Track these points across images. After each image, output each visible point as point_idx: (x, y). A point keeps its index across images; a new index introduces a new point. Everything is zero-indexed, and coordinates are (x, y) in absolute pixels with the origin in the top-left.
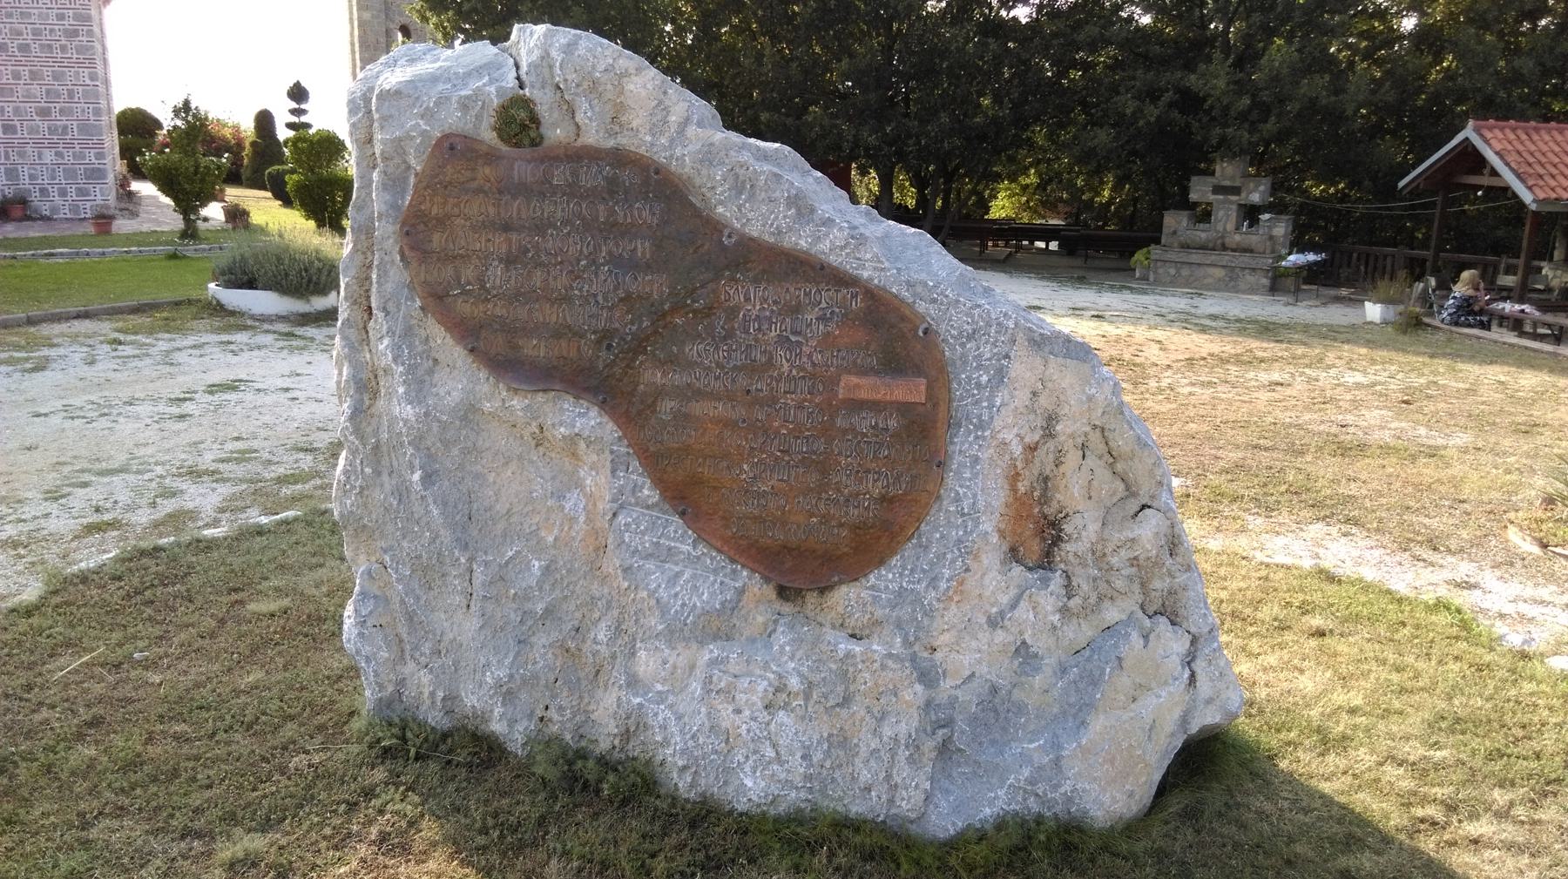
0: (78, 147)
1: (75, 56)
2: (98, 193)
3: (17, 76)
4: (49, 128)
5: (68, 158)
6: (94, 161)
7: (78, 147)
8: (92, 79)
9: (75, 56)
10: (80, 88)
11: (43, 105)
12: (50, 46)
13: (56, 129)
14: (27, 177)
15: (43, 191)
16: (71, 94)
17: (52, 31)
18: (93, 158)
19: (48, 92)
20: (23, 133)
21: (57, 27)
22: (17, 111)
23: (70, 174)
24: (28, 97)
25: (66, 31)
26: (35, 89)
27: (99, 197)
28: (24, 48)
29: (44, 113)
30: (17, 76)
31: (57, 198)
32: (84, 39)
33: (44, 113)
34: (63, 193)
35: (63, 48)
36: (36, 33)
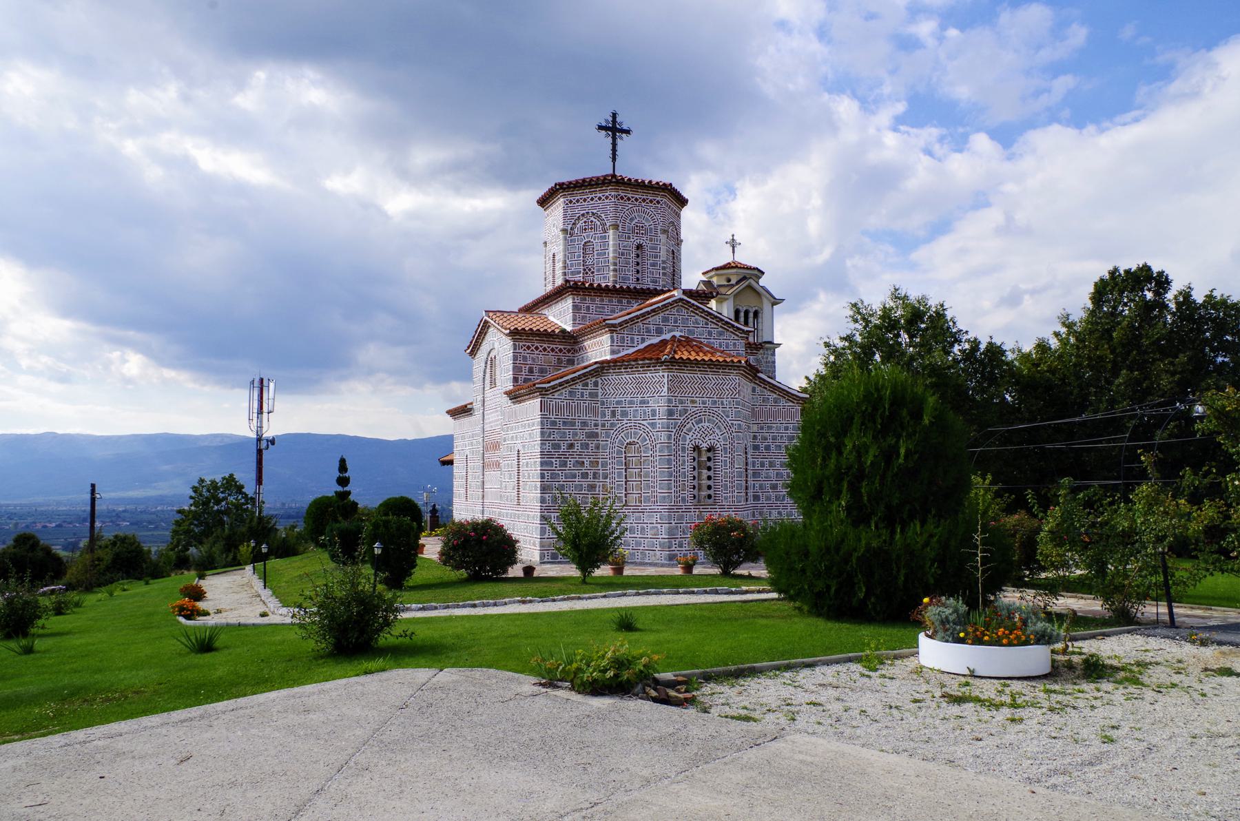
3: (762, 465)
19: (777, 474)
22: (761, 487)
28: (768, 448)
30: (762, 465)
36: (774, 438)
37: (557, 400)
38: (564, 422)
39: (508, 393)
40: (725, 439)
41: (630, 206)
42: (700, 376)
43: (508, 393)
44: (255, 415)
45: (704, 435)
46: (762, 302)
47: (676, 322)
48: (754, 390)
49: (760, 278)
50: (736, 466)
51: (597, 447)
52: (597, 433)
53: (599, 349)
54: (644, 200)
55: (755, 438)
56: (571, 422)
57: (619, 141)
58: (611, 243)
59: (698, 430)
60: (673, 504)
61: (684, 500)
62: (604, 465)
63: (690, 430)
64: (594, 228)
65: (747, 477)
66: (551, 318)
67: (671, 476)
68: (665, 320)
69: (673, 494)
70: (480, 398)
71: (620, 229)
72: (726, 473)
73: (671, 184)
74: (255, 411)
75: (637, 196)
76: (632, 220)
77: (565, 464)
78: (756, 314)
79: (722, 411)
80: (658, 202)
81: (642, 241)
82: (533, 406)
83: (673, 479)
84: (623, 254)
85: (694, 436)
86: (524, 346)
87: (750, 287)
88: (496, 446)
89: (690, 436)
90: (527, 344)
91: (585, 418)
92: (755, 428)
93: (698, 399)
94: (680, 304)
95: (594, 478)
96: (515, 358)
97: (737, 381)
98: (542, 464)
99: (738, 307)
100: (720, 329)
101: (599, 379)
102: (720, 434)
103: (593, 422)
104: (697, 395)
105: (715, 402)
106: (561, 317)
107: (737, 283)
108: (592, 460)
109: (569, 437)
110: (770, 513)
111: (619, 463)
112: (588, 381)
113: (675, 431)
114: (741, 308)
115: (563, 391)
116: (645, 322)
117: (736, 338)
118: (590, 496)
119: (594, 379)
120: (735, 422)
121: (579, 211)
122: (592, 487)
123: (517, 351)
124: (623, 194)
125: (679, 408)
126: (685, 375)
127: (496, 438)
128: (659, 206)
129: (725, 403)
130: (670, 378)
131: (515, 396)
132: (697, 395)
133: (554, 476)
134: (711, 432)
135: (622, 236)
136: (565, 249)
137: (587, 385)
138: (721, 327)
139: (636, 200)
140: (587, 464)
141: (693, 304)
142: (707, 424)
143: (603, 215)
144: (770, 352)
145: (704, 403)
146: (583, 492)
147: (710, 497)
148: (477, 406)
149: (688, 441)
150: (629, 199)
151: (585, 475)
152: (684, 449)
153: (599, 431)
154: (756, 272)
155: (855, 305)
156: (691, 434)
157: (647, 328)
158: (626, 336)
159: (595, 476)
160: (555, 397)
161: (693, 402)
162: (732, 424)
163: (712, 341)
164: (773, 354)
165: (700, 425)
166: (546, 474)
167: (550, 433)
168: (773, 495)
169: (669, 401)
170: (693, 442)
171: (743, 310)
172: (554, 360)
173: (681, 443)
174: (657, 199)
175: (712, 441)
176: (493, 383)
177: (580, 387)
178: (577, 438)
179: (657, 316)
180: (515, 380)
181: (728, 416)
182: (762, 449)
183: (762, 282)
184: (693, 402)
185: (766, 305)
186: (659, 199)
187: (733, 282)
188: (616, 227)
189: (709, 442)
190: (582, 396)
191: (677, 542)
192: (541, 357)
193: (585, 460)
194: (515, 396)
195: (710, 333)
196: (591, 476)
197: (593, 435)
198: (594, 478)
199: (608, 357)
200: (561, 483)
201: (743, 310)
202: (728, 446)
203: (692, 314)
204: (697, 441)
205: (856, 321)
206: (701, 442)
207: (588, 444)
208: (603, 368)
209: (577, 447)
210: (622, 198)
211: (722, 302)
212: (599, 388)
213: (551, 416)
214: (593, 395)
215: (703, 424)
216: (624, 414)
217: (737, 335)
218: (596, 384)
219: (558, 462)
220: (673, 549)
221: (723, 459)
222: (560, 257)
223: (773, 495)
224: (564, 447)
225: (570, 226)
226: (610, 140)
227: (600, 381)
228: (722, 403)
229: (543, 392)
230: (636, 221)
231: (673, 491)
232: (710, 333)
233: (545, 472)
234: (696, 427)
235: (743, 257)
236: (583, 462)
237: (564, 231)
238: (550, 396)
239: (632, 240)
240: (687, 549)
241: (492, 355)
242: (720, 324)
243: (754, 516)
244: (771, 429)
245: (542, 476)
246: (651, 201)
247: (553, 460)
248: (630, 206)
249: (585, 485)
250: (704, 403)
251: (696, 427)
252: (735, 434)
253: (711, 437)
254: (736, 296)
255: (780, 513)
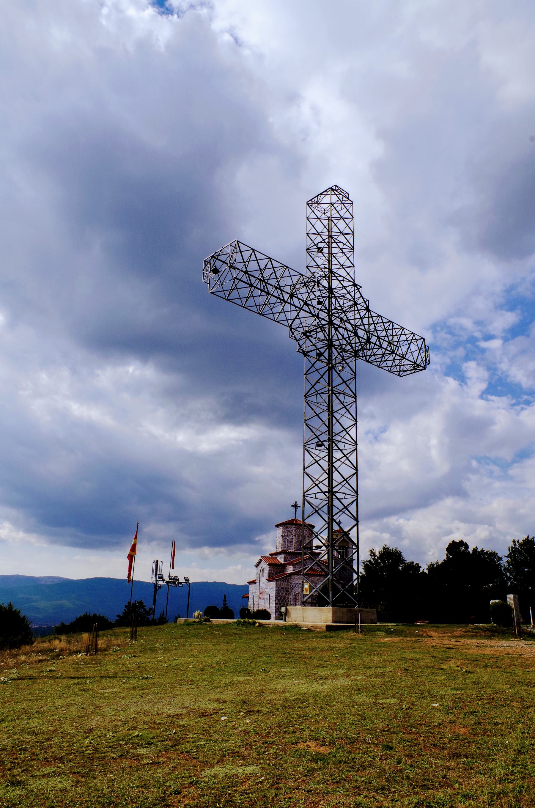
39: (267, 580)
43: (267, 580)
44: (154, 576)
51: (289, 594)
53: (290, 569)
62: (291, 598)
64: (290, 536)
66: (278, 559)
68: (306, 562)
70: (258, 579)
74: (154, 574)
77: (281, 598)
82: (274, 584)
88: (263, 593)
96: (269, 570)
98: (276, 598)
106: (281, 559)
109: (282, 591)
111: (294, 598)
121: (286, 531)
127: (263, 591)
131: (269, 580)
133: (278, 601)
136: (282, 539)
148: (257, 581)
155: (371, 551)
159: (288, 601)
164: (353, 563)
172: (279, 571)
176: (263, 576)
180: (269, 576)
188: (295, 536)
192: (275, 569)
194: (269, 580)
197: (288, 591)
199: (292, 572)
205: (371, 556)
208: (291, 574)
209: (284, 594)
214: (288, 581)
216: (296, 586)
218: (289, 578)
222: (281, 542)
229: (276, 581)
237: (282, 536)
241: (263, 568)
245: (276, 601)
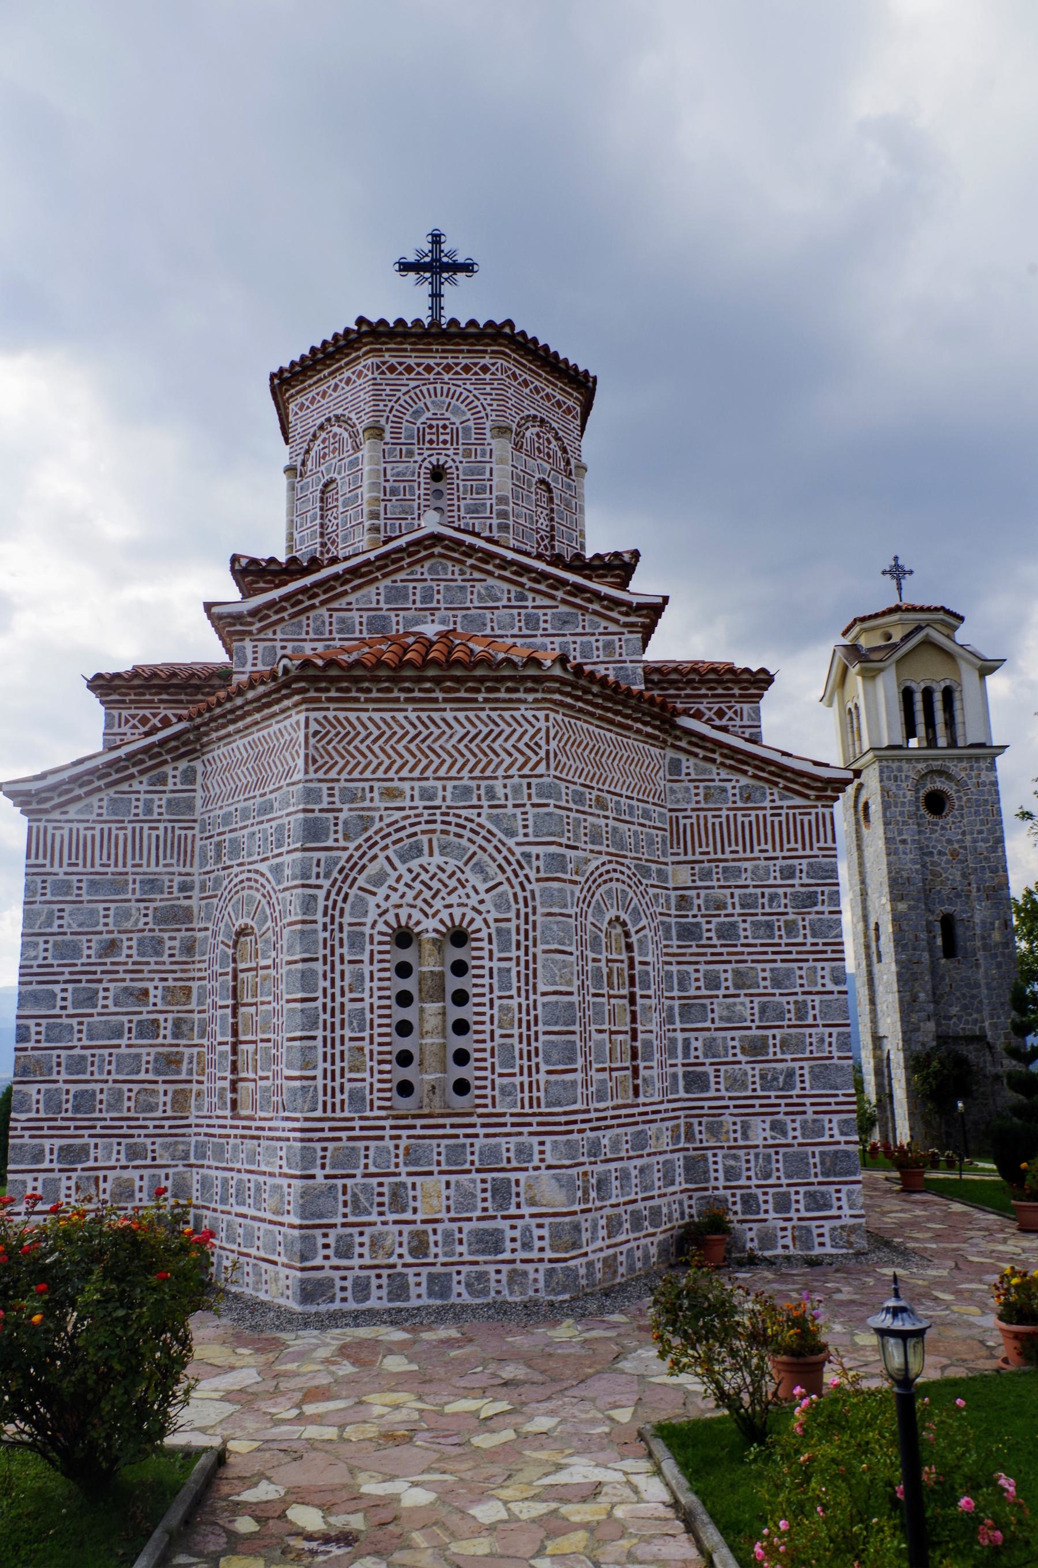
0: (810, 1110)
1: (810, 940)
2: (844, 1203)
3: (713, 982)
4: (763, 1077)
5: (795, 1133)
6: (838, 1137)
7: (810, 1110)
8: (837, 981)
9: (810, 940)
10: (817, 998)
11: (754, 1032)
12: (769, 926)
13: (776, 1079)
14: (721, 1175)
15: (749, 1203)
16: (801, 1010)
17: (773, 898)
18: (836, 1131)
20: (718, 1088)
21: (781, 891)
22: (710, 1047)
23: (797, 1165)
24: (729, 1020)
25: (795, 896)
26: (745, 1006)
27: (846, 1211)
28: (727, 932)
29: (756, 1048)
30: (713, 982)
31: (772, 1215)
32: (826, 909)
33: (756, 1048)
34: (783, 1204)
35: (791, 928)
37: (75, 826)
38: (92, 883)
40: (501, 904)
41: (413, 384)
42: (413, 716)
45: (427, 894)
46: (958, 671)
47: (427, 597)
48: (675, 767)
49: (955, 628)
50: (542, 988)
52: (188, 910)
54: (448, 368)
55: (683, 902)
56: (112, 882)
57: (446, 289)
58: (366, 468)
59: (407, 878)
60: (319, 1113)
61: (357, 1098)
63: (379, 879)
65: (634, 1020)
67: (314, 1025)
68: (396, 595)
69: (320, 1082)
71: (387, 436)
72: (505, 1010)
73: (509, 323)
75: (431, 362)
76: (417, 413)
77: (91, 999)
78: (948, 694)
79: (490, 817)
80: (485, 369)
81: (450, 463)
83: (319, 1033)
84: (394, 492)
85: (395, 898)
86: (133, 717)
87: (928, 643)
89: (379, 899)
90: (141, 712)
91: (153, 869)
92: (683, 876)
93: (406, 786)
94: (437, 550)
95: (176, 1036)
97: (542, 724)
98: (23, 999)
99: (908, 684)
100: (564, 609)
101: (198, 764)
102: (482, 887)
103: (177, 879)
104: (404, 773)
105: (467, 791)
107: (906, 638)
108: (170, 983)
110: (746, 1128)
112: (168, 769)
113: (326, 883)
114: (913, 685)
115: (94, 800)
116: (335, 605)
117: (613, 628)
118: (161, 1088)
119: (183, 764)
120: (534, 850)
122: (170, 1062)
123: (116, 730)
124: (394, 361)
125: (342, 816)
126: (364, 716)
128: (488, 376)
129: (500, 792)
130: (314, 726)
132: (404, 773)
133: (56, 1033)
134: (452, 883)
135: (391, 452)
137: (162, 780)
138: (564, 601)
139: (429, 369)
140: (156, 995)
141: (471, 547)
142: (438, 859)
143: (353, 415)
144: (983, 765)
145: (427, 795)
146: (142, 1076)
147: (462, 1087)
149: (373, 914)
150: (409, 369)
151: (149, 1029)
152: (357, 940)
153: (194, 903)
154: (941, 616)
156: (382, 891)
157: (342, 621)
158: (278, 644)
160: (72, 816)
161: (390, 794)
162: (527, 856)
163: (538, 640)
164: (993, 768)
165: (414, 864)
166: (33, 1029)
167: (51, 913)
168: (753, 1072)
169: (311, 795)
170: (390, 917)
171: (918, 688)
173: (347, 919)
174: (482, 362)
175: (457, 912)
177: (144, 787)
178: (128, 925)
179: (372, 589)
181: (511, 833)
182: (709, 929)
183: (962, 635)
184: (390, 794)
185: (969, 677)
186: (487, 361)
187: (896, 639)
189: (444, 915)
190: (149, 811)
191: (331, 1240)
193: (150, 985)
195: (532, 622)
196: (166, 1030)
198: (176, 1036)
200: (77, 1052)
201: (918, 688)
202: (512, 925)
203: (477, 575)
204: (403, 913)
206: (417, 915)
207: (161, 942)
209: (129, 950)
210: (392, 369)
211: (874, 677)
212: (197, 786)
213: (56, 869)
214: (182, 807)
215: (424, 860)
217: (616, 621)
218: (189, 777)
219: (68, 995)
220: (318, 1261)
221: (496, 965)
223: (753, 1072)
224: (89, 951)
225: (300, 458)
226: (426, 288)
227: (200, 768)
228: (491, 794)
230: (429, 415)
231: (319, 1073)
232: (532, 622)
233: (31, 1023)
234: (402, 868)
235: (915, 594)
236: (145, 992)
237: (290, 470)
238: (56, 815)
239: (419, 458)
240: (367, 1261)
242: (560, 594)
243: (690, 1137)
244: (738, 872)
245: (22, 1035)
246: (467, 369)
247: (57, 988)
248: (413, 384)
249: (148, 1054)
250: (427, 795)
251: (402, 868)
252: (536, 886)
253: (453, 899)
254: (898, 662)
255: (778, 1127)
